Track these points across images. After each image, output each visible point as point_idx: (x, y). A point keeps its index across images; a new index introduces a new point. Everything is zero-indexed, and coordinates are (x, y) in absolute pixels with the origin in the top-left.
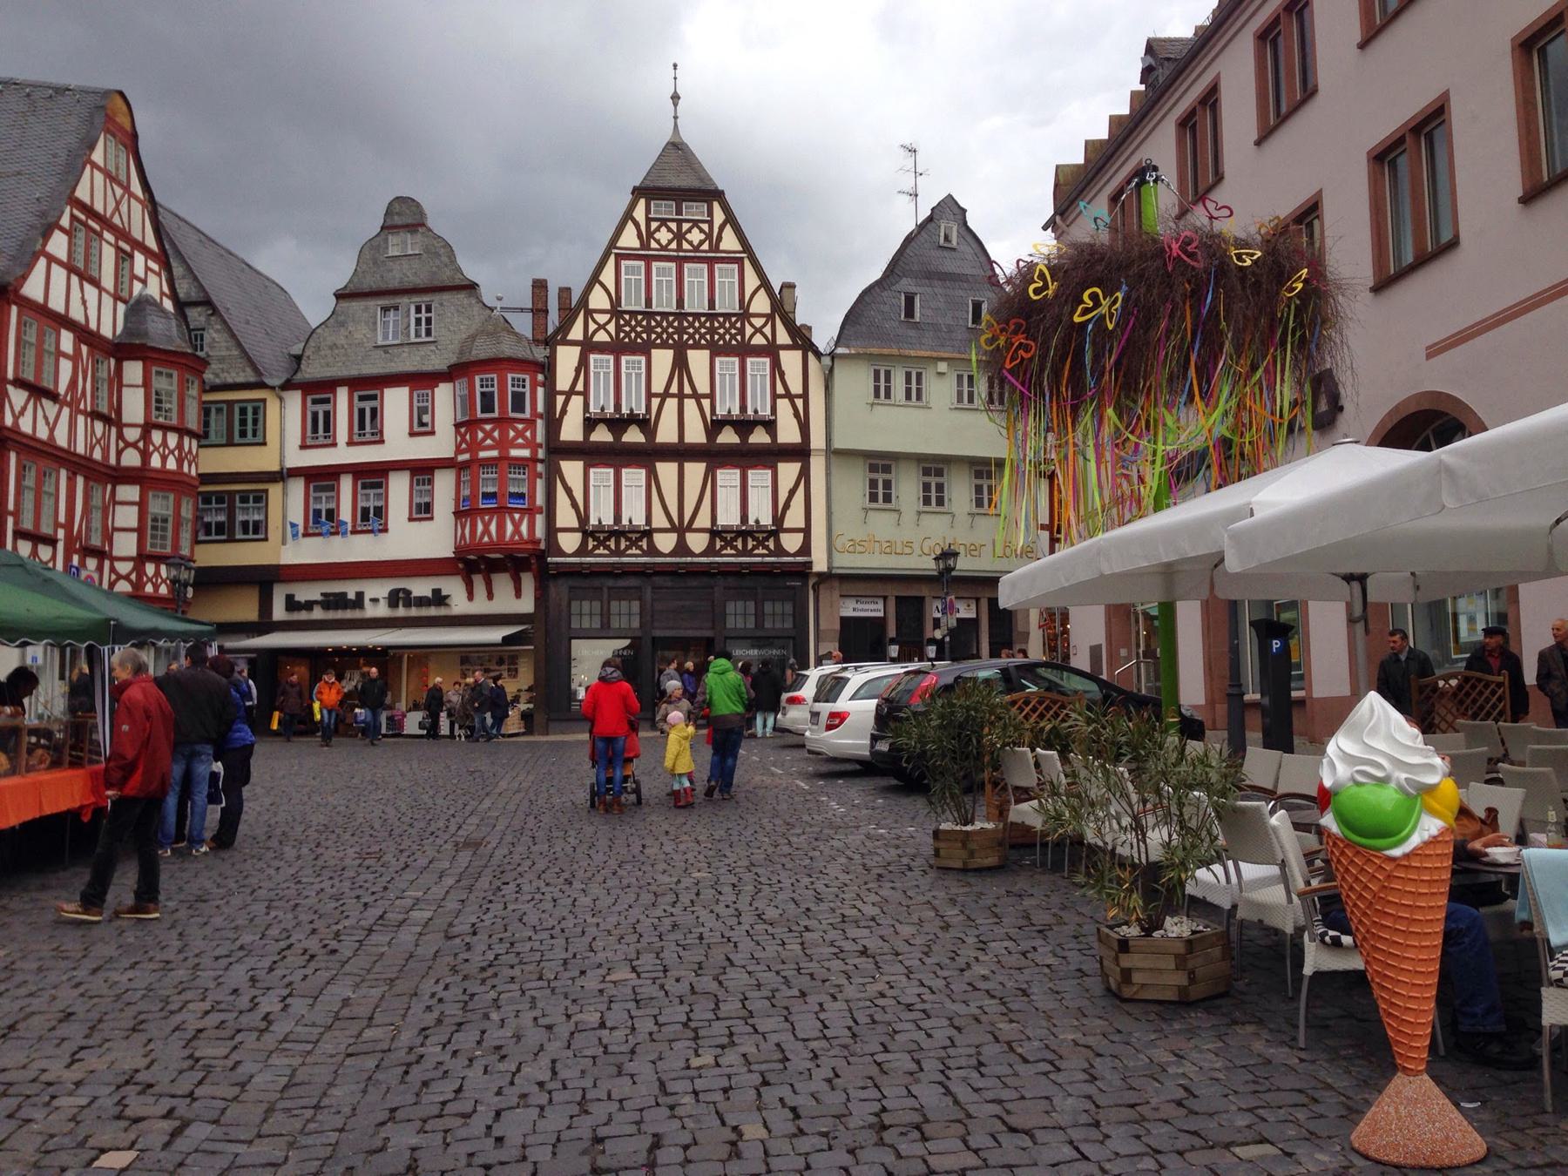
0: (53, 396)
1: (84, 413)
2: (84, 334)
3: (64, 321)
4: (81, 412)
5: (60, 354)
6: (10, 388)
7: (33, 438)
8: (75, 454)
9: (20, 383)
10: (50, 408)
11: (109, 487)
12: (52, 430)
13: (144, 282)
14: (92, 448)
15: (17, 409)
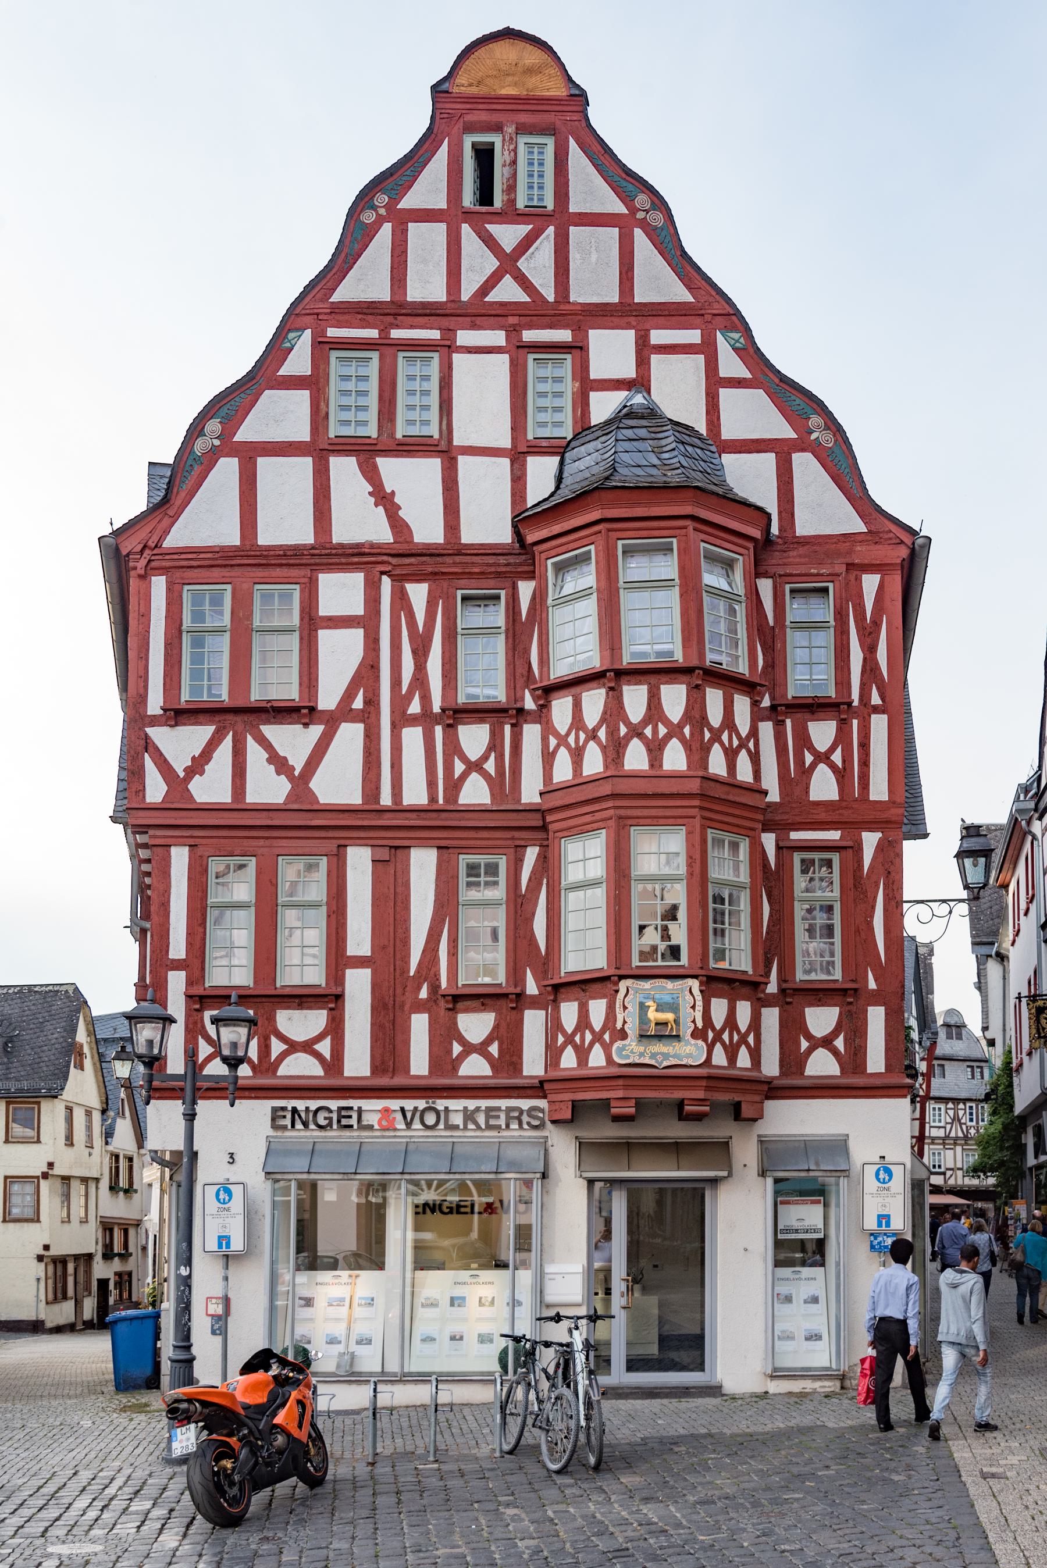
0: (300, 712)
1: (426, 719)
2: (397, 559)
3: (326, 555)
4: (413, 721)
5: (312, 623)
6: (155, 733)
7: (239, 804)
8: (398, 809)
9: (178, 715)
10: (294, 741)
11: (531, 854)
12: (301, 781)
13: (641, 382)
14: (454, 786)
15: (180, 765)
